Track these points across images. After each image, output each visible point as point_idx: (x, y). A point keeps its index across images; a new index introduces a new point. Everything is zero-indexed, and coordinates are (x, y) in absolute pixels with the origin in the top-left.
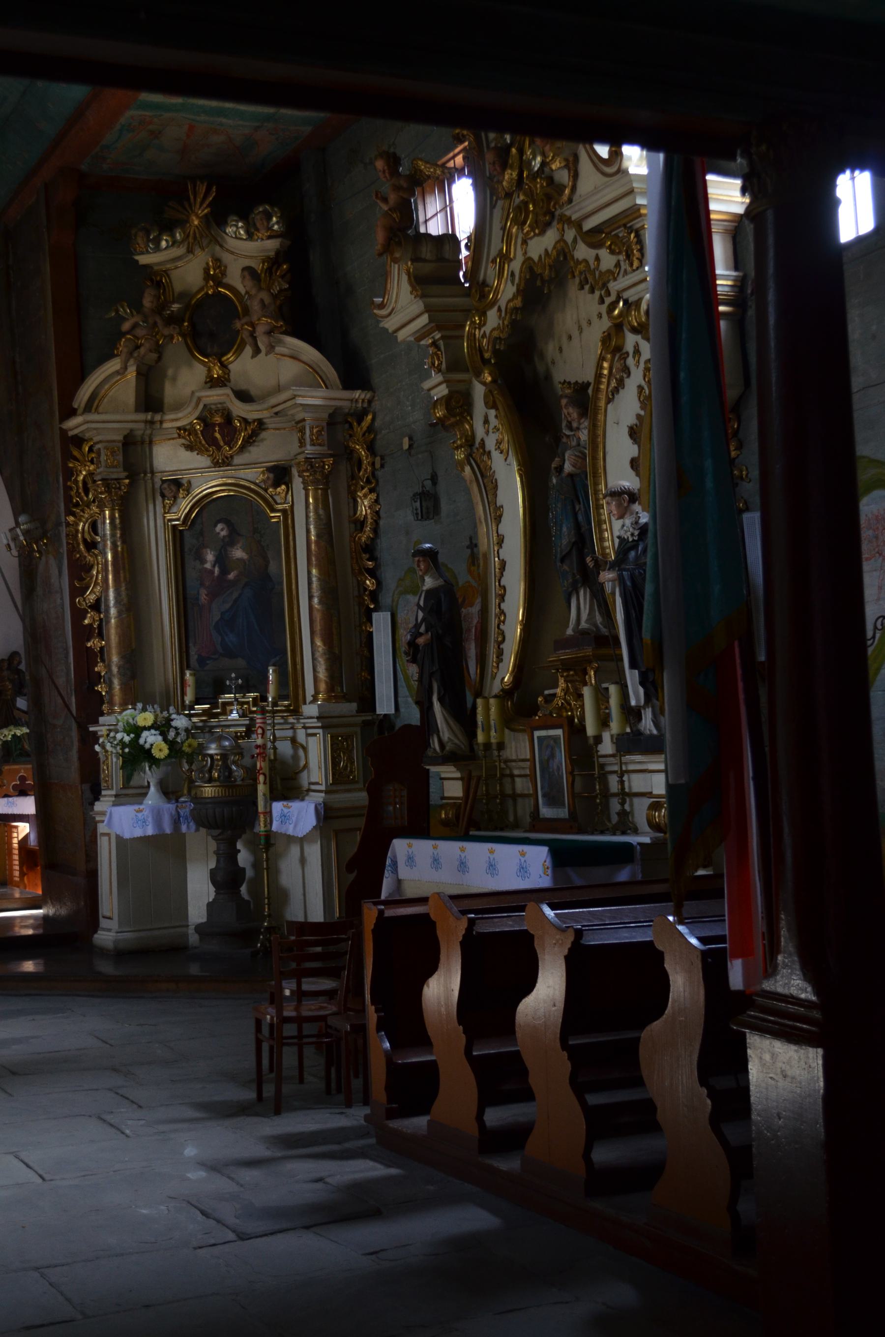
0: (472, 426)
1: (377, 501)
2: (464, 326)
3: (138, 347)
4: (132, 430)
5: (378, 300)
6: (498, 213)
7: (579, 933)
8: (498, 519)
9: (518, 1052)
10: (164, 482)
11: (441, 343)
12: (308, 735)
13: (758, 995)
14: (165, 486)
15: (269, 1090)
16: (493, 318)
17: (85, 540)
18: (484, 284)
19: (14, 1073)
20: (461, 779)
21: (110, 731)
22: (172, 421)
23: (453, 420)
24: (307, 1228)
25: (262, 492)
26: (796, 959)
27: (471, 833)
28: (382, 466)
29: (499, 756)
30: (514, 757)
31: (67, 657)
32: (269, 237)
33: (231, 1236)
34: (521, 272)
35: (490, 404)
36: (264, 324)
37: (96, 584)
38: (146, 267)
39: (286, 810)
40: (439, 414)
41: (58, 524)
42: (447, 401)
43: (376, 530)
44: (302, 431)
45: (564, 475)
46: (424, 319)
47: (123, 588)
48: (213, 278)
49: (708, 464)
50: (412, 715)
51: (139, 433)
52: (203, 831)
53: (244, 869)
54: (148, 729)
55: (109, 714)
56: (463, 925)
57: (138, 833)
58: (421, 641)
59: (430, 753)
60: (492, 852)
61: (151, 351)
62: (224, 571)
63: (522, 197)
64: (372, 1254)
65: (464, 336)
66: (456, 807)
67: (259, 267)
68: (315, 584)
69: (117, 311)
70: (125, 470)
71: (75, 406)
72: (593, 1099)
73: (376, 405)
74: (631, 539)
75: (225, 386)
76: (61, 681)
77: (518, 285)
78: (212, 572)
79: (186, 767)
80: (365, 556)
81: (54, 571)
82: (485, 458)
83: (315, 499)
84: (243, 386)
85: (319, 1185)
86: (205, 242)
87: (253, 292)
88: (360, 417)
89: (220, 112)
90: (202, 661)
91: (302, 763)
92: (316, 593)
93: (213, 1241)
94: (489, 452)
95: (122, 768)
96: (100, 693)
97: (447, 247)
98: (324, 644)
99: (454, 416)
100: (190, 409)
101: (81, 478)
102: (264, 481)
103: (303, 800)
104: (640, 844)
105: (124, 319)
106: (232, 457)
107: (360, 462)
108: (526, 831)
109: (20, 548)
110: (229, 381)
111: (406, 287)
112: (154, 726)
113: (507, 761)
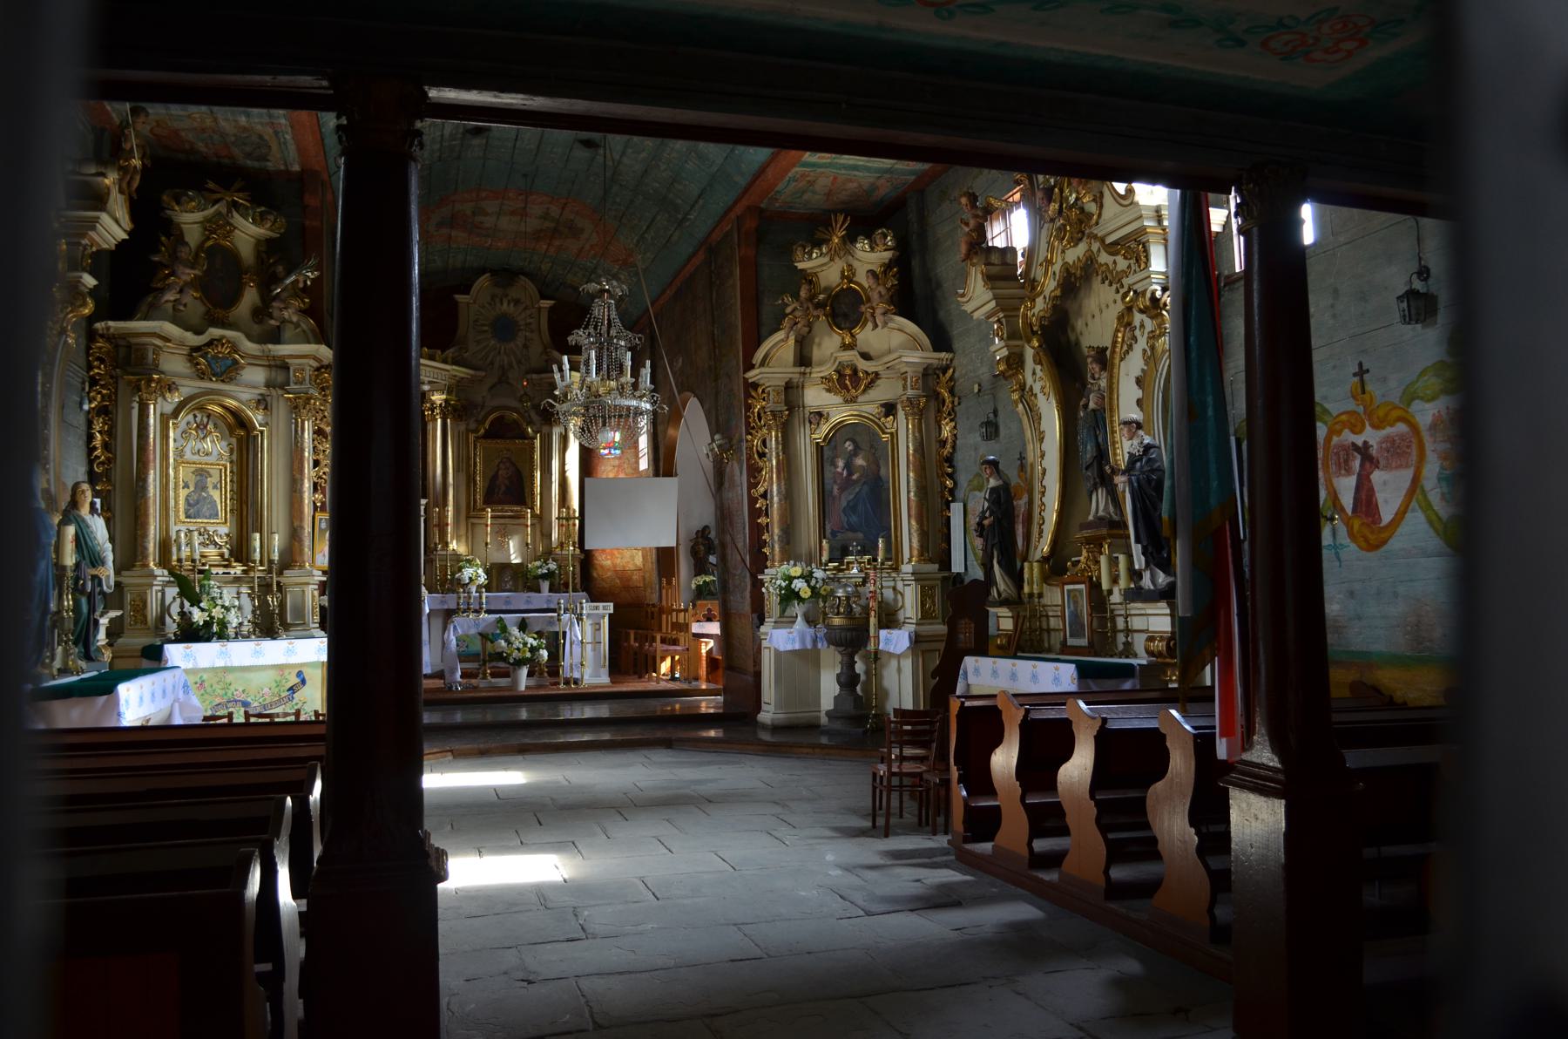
0: (1024, 377)
1: (955, 427)
3: (796, 324)
4: (791, 379)
5: (961, 291)
6: (1044, 232)
7: (1105, 720)
8: (1042, 440)
9: (1060, 802)
10: (811, 413)
11: (1004, 320)
12: (905, 585)
13: (1238, 762)
14: (812, 416)
15: (881, 821)
16: (1040, 304)
17: (758, 452)
18: (1034, 280)
19: (710, 801)
20: (1012, 617)
21: (772, 579)
22: (818, 372)
23: (1010, 372)
24: (912, 910)
25: (877, 420)
26: (1267, 738)
27: (1018, 654)
28: (959, 404)
29: (1039, 602)
30: (1049, 604)
31: (744, 528)
32: (885, 250)
33: (862, 913)
34: (1060, 272)
35: (1038, 361)
37: (765, 480)
38: (802, 270)
39: (889, 635)
40: (1002, 367)
41: (741, 441)
42: (1007, 359)
43: (954, 447)
44: (905, 380)
45: (1089, 410)
46: (993, 304)
47: (783, 484)
48: (847, 277)
49: (1210, 399)
50: (979, 574)
51: (795, 381)
52: (832, 647)
53: (859, 675)
54: (798, 578)
55: (771, 567)
56: (1022, 712)
57: (789, 647)
58: (986, 522)
59: (990, 599)
60: (1034, 667)
61: (804, 326)
62: (850, 474)
63: (1062, 222)
64: (956, 930)
65: (1019, 316)
66: (1009, 637)
67: (878, 270)
68: (912, 484)
69: (783, 300)
70: (786, 405)
71: (754, 363)
72: (1111, 836)
73: (956, 363)
74: (1137, 454)
75: (853, 349)
76: (740, 545)
77: (1058, 281)
78: (842, 474)
79: (821, 604)
80: (946, 465)
81: (737, 472)
82: (1033, 398)
83: (913, 426)
85: (918, 884)
86: (842, 253)
87: (874, 286)
88: (945, 370)
89: (855, 168)
90: (834, 534)
91: (900, 604)
92: (913, 489)
93: (848, 915)
95: (779, 604)
96: (766, 553)
97: (1009, 256)
100: (828, 366)
101: (757, 410)
102: (879, 414)
103: (900, 629)
104: (1139, 665)
105: (787, 305)
107: (944, 401)
108: (1057, 654)
109: (715, 456)
110: (856, 346)
111: (980, 283)
112: (801, 577)
113: (1044, 606)
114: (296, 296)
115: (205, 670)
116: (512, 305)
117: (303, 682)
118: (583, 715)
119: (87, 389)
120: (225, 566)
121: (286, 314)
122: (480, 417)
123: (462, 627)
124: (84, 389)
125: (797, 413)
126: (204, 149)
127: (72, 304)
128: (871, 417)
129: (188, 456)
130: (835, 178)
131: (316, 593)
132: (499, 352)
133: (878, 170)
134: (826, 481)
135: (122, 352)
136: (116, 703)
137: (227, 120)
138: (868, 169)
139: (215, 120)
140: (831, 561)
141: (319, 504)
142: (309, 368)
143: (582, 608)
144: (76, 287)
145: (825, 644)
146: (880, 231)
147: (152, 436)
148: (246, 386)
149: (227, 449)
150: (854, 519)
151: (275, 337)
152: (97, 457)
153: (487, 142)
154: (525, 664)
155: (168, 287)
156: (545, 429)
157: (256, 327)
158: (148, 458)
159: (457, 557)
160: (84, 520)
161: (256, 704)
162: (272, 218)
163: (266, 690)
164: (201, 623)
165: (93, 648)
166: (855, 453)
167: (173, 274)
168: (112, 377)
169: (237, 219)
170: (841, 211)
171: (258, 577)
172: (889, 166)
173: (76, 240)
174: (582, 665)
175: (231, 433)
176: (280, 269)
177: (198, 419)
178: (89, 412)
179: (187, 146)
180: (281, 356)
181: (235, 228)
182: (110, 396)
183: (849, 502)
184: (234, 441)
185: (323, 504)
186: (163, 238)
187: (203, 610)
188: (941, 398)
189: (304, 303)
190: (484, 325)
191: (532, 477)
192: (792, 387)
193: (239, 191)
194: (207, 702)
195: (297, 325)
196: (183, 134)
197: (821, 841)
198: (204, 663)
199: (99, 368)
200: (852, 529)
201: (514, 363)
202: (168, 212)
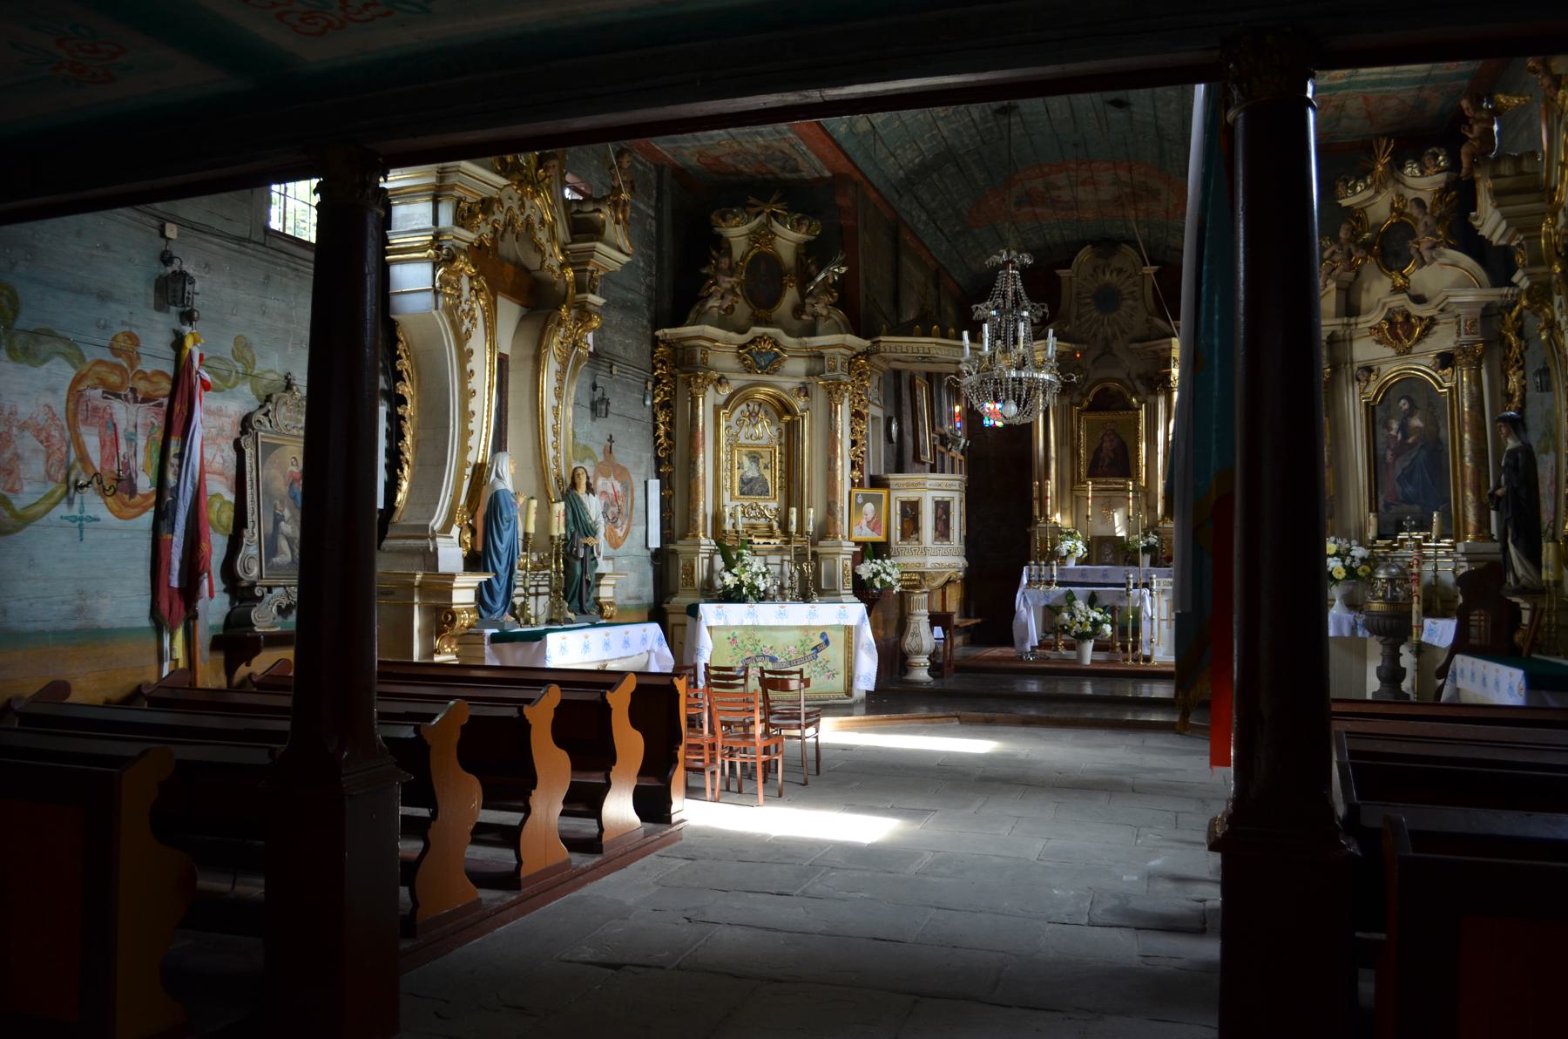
1: (1524, 377)
2: (1541, 228)
3: (1334, 269)
5: (1473, 214)
10: (1359, 368)
19: (1133, 791)
25: (1433, 374)
32: (1437, 172)
36: (1426, 241)
38: (1349, 208)
39: (1433, 626)
44: (1458, 323)
46: (1503, 225)
53: (1405, 669)
58: (1499, 492)
61: (1345, 270)
62: (1405, 437)
65: (1540, 237)
78: (1396, 437)
83: (1469, 377)
84: (1419, 291)
85: (1201, 904)
88: (1510, 307)
90: (1387, 506)
93: (1067, 921)
94: (1563, 333)
98: (1474, 494)
99: (1536, 303)
106: (1411, 347)
107: (1510, 346)
110: (1409, 288)
112: (1337, 554)
114: (827, 292)
115: (736, 627)
116: (1115, 274)
117: (827, 642)
118: (1152, 693)
119: (650, 387)
120: (770, 537)
121: (820, 309)
122: (1084, 390)
123: (1032, 599)
124: (646, 388)
125: (1343, 370)
126: (746, 170)
127: (581, 320)
128: (1428, 370)
129: (742, 440)
130: (1366, 99)
131: (849, 563)
132: (1103, 324)
133: (1414, 81)
134: (1380, 446)
135: (680, 355)
136: (543, 648)
137: (748, 142)
138: (1401, 82)
139: (740, 143)
140: (1380, 536)
141: (857, 481)
142: (839, 357)
143: (1152, 583)
144: (584, 306)
145: (1367, 634)
146: (1430, 151)
147: (701, 424)
148: (787, 376)
149: (777, 434)
150: (1410, 489)
151: (812, 331)
152: (661, 444)
153: (1022, 120)
154: (1090, 638)
155: (710, 295)
156: (1151, 399)
157: (797, 322)
158: (697, 443)
159: (1058, 530)
160: (579, 498)
161: (782, 660)
162: (807, 222)
163: (792, 648)
164: (732, 586)
165: (587, 605)
166: (1410, 413)
167: (715, 283)
168: (672, 376)
169: (777, 227)
170: (1383, 136)
171: (796, 548)
172: (1425, 74)
173: (582, 268)
174: (1152, 642)
175: (780, 418)
176: (813, 268)
177: (751, 408)
178: (653, 405)
179: (733, 169)
180: (818, 347)
181: (776, 235)
182: (671, 393)
183: (1403, 470)
184: (783, 426)
185: (861, 480)
186: (714, 253)
187: (735, 575)
188: (1506, 341)
189: (832, 296)
190: (1085, 298)
191: (1137, 449)
192: (1338, 341)
193: (776, 202)
194: (739, 656)
195: (828, 318)
196: (723, 159)
197: (1177, 844)
198: (734, 622)
199: (662, 369)
200: (1407, 500)
201: (1118, 334)
202: (717, 229)
